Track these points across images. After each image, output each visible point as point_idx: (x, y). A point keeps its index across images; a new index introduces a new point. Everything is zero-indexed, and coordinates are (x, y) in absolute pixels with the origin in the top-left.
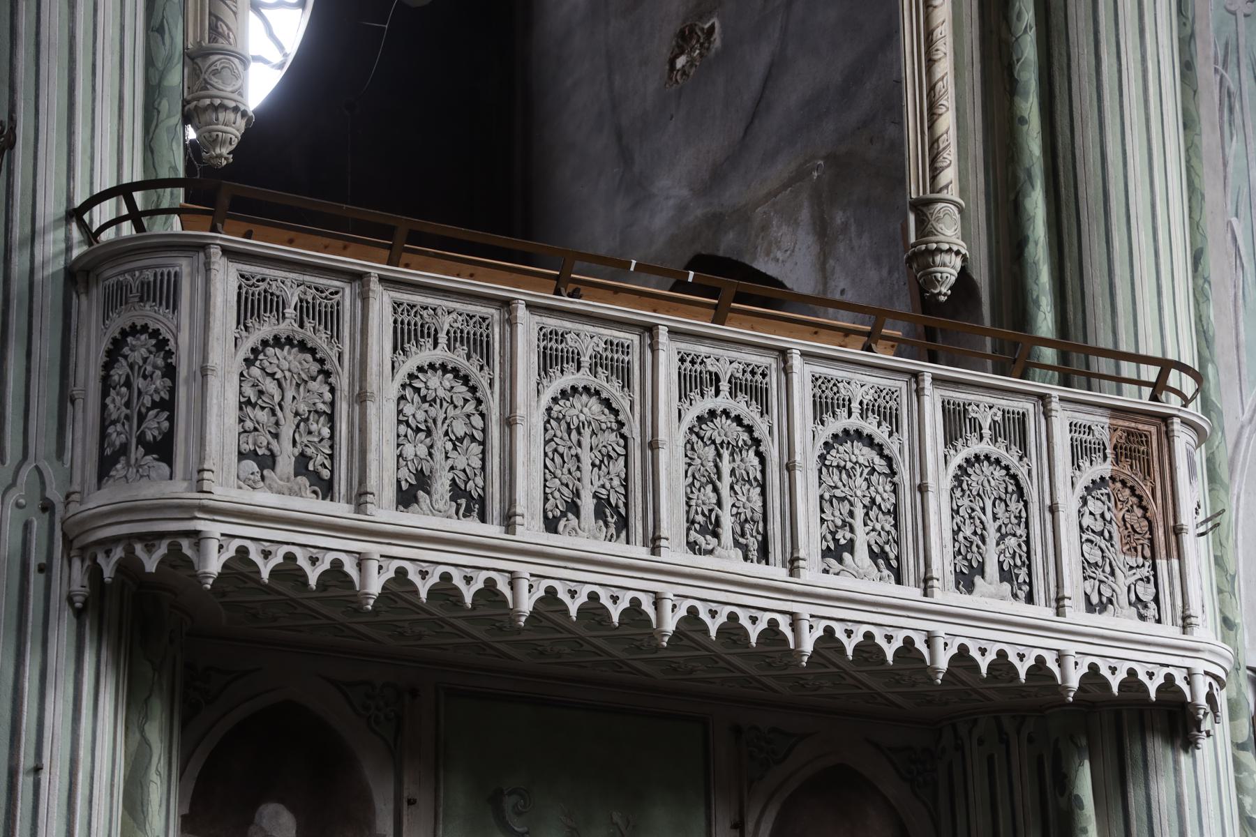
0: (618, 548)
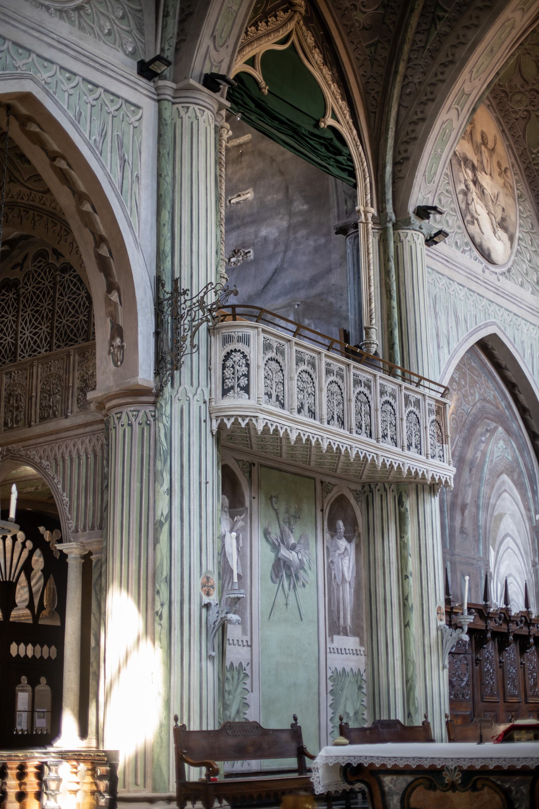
0: (341, 430)
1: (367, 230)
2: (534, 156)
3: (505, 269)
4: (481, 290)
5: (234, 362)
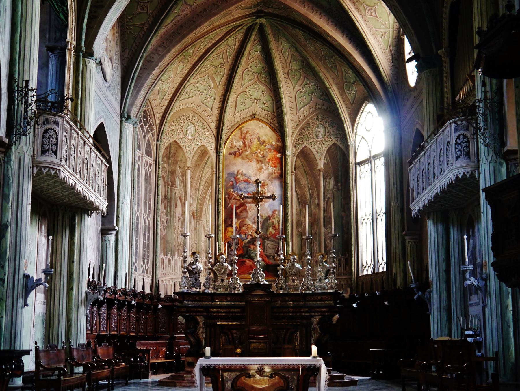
1: (71, 55)
2: (127, 20)
3: (108, 85)
4: (101, 96)
5: (50, 135)
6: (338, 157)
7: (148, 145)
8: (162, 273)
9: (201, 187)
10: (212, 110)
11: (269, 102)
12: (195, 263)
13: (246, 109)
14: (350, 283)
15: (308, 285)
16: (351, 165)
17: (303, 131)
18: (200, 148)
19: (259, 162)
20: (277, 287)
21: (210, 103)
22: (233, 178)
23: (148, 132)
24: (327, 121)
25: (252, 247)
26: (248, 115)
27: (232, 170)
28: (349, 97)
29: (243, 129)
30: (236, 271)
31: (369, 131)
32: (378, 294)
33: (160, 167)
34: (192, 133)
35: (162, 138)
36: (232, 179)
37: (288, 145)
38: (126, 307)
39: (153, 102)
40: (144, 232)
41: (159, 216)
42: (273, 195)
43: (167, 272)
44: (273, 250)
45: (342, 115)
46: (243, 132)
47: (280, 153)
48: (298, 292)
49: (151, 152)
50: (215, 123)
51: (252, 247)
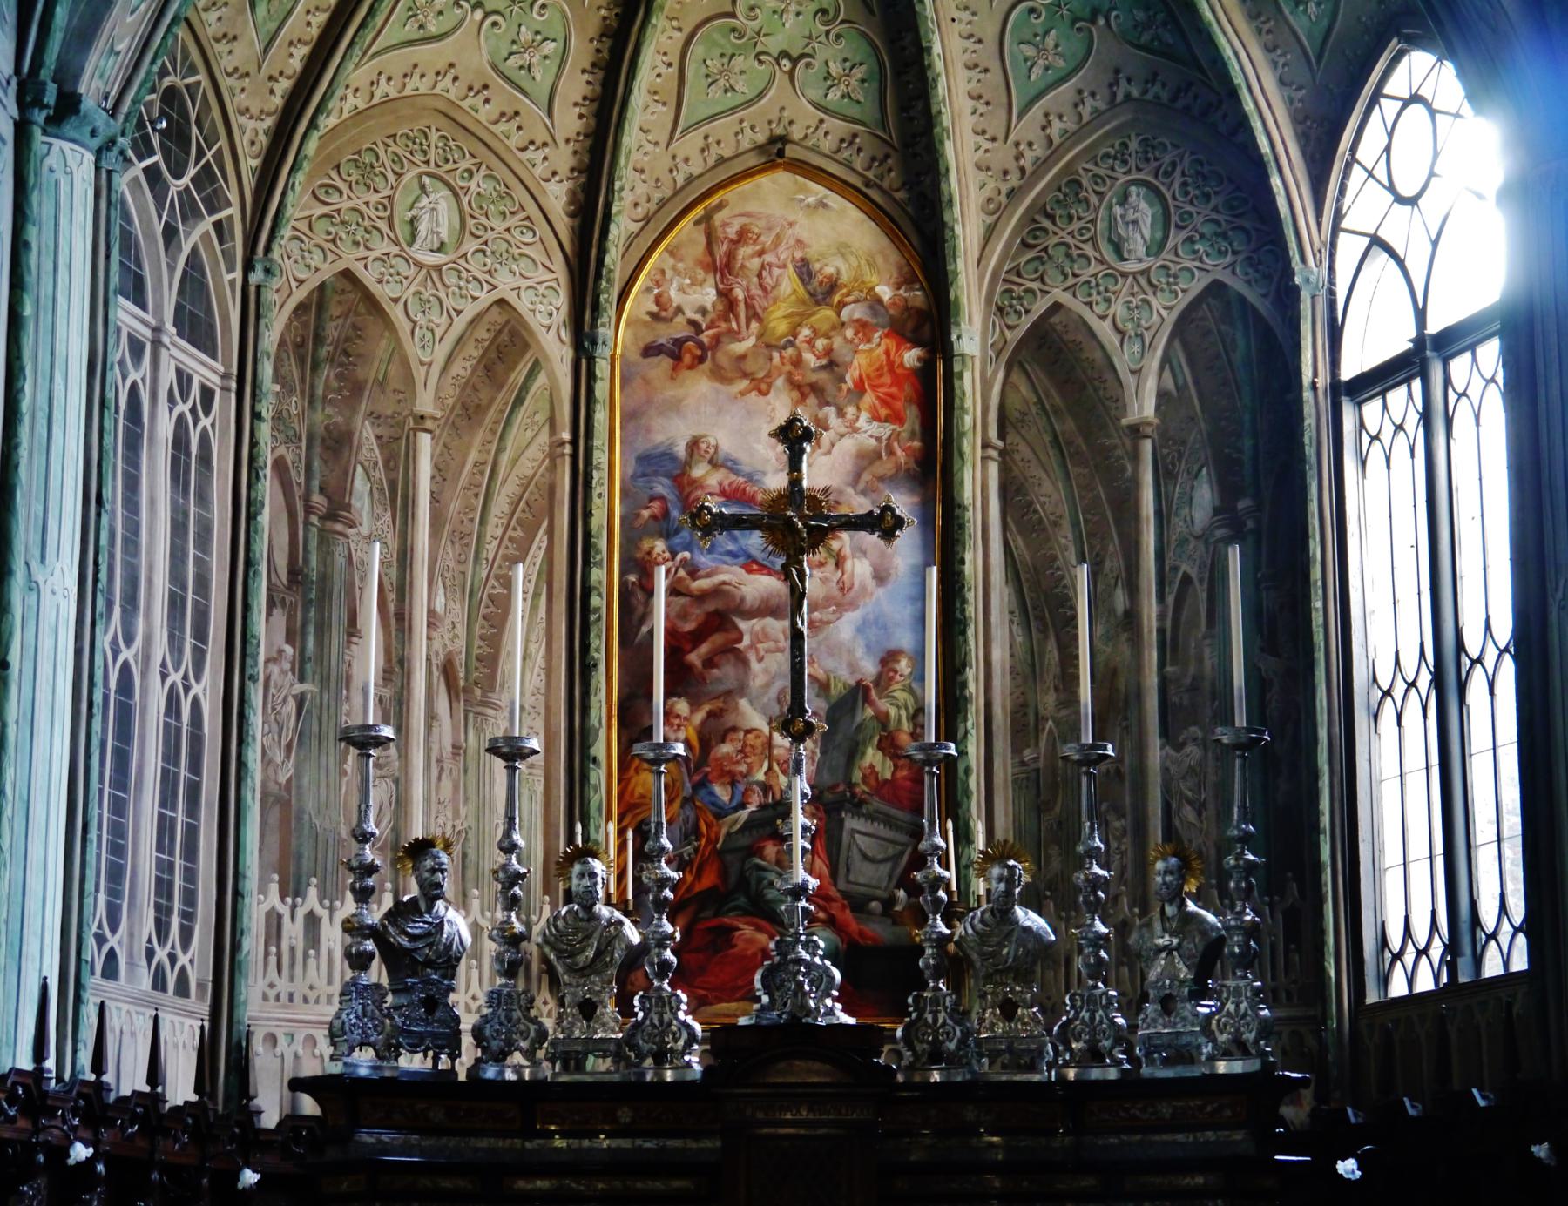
6: (1238, 357)
7: (193, 282)
8: (272, 993)
9: (494, 528)
10: (550, 113)
11: (859, 73)
12: (423, 907)
13: (733, 110)
14: (1311, 1042)
15: (1093, 1032)
16: (1307, 395)
17: (1046, 223)
18: (486, 319)
19: (804, 396)
20: (911, 1047)
21: (542, 77)
22: (666, 481)
23: (191, 212)
24: (1174, 164)
25: (771, 850)
26: (746, 145)
27: (659, 438)
28: (1300, 23)
29: (719, 218)
30: (668, 954)
31: (1412, 201)
32: (1482, 1103)
33: (266, 409)
34: (444, 235)
35: (276, 254)
36: (662, 487)
37: (964, 300)
38: (41, 1181)
39: (221, 47)
40: (166, 758)
41: (253, 679)
42: (887, 508)
43: (300, 988)
44: (885, 868)
45: (1257, 125)
46: (720, 234)
47: (916, 343)
48: (1036, 1078)
49: (212, 327)
50: (567, 185)
51: (771, 850)
